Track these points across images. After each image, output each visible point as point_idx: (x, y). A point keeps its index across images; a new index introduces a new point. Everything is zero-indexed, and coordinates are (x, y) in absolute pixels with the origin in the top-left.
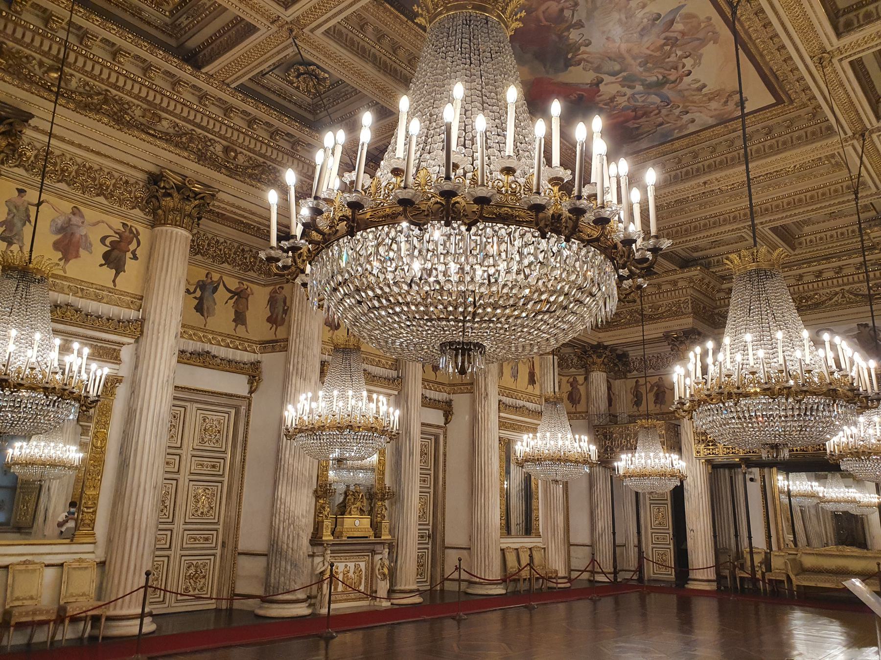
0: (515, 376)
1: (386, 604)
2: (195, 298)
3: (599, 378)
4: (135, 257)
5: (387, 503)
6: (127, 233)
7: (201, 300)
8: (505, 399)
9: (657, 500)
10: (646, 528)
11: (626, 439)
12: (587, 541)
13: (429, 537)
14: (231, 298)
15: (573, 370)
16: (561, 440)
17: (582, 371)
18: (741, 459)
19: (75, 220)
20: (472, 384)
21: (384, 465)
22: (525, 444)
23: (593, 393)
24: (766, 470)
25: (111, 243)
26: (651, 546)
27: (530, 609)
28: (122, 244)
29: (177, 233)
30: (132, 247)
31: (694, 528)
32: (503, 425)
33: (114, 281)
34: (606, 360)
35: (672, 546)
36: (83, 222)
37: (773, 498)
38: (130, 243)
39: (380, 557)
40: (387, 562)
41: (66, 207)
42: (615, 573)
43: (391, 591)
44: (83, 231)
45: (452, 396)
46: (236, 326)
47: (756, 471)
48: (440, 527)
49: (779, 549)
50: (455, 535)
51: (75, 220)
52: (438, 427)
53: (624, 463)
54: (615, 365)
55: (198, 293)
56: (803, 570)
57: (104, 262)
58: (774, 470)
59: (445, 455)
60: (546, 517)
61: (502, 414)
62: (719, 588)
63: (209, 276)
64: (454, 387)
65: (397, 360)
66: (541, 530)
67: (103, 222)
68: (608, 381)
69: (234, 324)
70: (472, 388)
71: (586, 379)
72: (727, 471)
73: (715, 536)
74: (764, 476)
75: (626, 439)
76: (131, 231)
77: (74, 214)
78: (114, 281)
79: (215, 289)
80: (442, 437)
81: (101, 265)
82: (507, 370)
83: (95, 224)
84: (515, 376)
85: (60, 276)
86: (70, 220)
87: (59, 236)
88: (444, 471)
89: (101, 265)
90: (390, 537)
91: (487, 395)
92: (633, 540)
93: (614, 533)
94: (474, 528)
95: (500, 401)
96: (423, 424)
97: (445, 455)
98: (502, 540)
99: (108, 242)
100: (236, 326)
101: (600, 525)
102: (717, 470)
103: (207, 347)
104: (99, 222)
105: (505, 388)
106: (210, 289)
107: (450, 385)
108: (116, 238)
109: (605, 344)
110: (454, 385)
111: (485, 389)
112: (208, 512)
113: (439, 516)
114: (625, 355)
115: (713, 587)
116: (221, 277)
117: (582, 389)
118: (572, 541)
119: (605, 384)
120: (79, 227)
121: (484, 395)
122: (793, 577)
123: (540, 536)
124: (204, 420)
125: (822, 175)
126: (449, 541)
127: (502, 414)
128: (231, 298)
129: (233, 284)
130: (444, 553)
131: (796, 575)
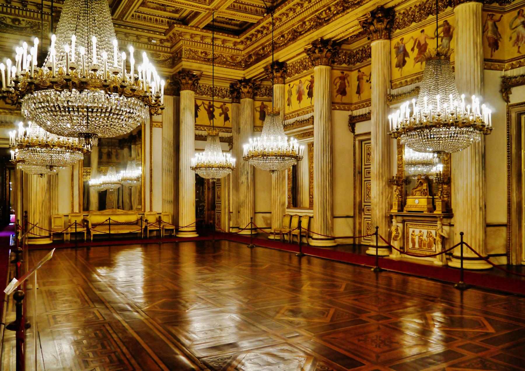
19: (300, 85)
51: (300, 85)
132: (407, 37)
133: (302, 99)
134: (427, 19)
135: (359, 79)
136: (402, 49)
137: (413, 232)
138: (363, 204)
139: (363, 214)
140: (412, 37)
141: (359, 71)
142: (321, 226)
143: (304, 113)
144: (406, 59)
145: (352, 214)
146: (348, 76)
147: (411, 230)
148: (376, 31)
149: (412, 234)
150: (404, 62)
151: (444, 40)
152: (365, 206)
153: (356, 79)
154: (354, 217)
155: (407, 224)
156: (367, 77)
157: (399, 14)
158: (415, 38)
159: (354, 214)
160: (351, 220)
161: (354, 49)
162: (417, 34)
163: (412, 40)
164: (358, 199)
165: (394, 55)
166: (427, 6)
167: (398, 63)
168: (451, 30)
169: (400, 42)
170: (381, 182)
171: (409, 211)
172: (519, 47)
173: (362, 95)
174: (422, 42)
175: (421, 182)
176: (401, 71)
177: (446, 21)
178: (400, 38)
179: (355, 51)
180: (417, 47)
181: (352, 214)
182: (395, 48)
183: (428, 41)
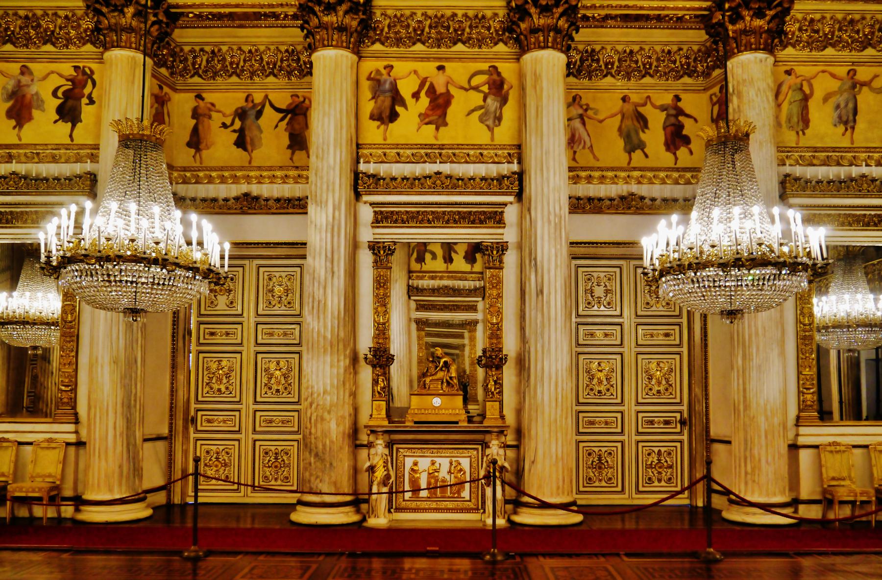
2: (234, 131)
4: (92, 102)
6: (80, 77)
7: (241, 132)
13: (683, 422)
14: (282, 119)
19: (25, 80)
25: (64, 93)
28: (76, 91)
29: (116, 56)
30: (87, 91)
33: (71, 136)
36: (32, 80)
38: (84, 86)
41: (14, 68)
44: (34, 89)
46: (293, 154)
51: (25, 80)
55: (238, 124)
57: (58, 117)
63: (250, 99)
67: (53, 72)
69: (289, 151)
76: (84, 73)
77: (22, 73)
78: (71, 136)
79: (259, 114)
81: (55, 122)
83: (45, 78)
85: (18, 145)
86: (19, 81)
87: (9, 104)
89: (55, 122)
99: (60, 94)
100: (293, 154)
103: (244, 188)
104: (48, 74)
106: (252, 114)
108: (68, 86)
112: (667, 390)
116: (266, 97)
120: (28, 86)
124: (270, 279)
128: (282, 119)
129: (282, 99)
130: (708, 450)
132: (401, 68)
133: (30, 118)
134: (410, 49)
135: (196, 114)
136: (387, 86)
137: (416, 464)
138: (193, 406)
139: (192, 430)
140: (415, 72)
141: (199, 97)
142: (120, 467)
143: (38, 158)
144: (398, 109)
145: (165, 431)
146: (169, 99)
147: (409, 462)
148: (341, 29)
149: (412, 470)
150: (393, 116)
151: (489, 100)
152: (198, 410)
153: (190, 114)
154: (169, 439)
155: (397, 449)
156: (224, 115)
157: (384, 14)
158: (423, 74)
159: (171, 431)
160: (161, 445)
161: (187, 44)
162: (428, 69)
163: (413, 76)
164: (181, 394)
165: (366, 93)
166: (413, 24)
167: (375, 112)
168: (505, 87)
169: (384, 72)
170: (342, 358)
171: (416, 423)
172: (575, 152)
173: (205, 153)
174: (440, 89)
175: (445, 362)
176: (386, 130)
177: (495, 68)
178: (386, 63)
179: (187, 49)
180: (428, 94)
181: (165, 431)
182: (369, 78)
183: (453, 91)
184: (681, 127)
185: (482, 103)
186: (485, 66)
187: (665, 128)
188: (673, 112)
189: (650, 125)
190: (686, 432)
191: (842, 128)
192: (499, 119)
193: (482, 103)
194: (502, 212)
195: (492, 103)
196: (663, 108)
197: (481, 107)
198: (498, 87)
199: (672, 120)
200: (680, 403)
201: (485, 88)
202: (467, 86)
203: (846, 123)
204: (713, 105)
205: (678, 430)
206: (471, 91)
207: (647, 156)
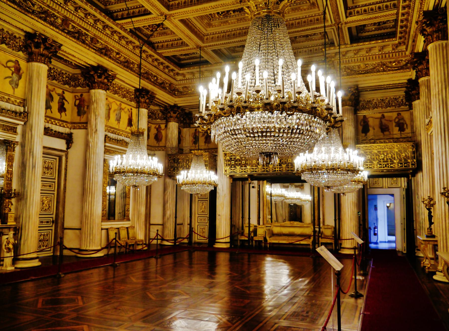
0: (118, 120)
1: (10, 268)
3: (173, 126)
5: (13, 201)
8: (110, 135)
9: (202, 198)
10: (195, 214)
11: (186, 163)
12: (160, 222)
13: (53, 222)
15: (159, 120)
16: (144, 161)
17: (164, 121)
18: (249, 175)
20: (86, 123)
21: (11, 174)
22: (115, 162)
23: (170, 135)
24: (261, 182)
26: (197, 224)
27: (114, 267)
31: (221, 214)
32: (107, 151)
34: (178, 116)
35: (208, 224)
37: (263, 197)
39: (7, 237)
40: (12, 241)
42: (175, 239)
43: (15, 260)
45: (72, 131)
47: (256, 182)
48: (61, 216)
49: (264, 224)
50: (70, 221)
52: (61, 151)
53: (182, 176)
54: (184, 119)
56: (273, 235)
58: (265, 182)
59: (66, 169)
60: (134, 210)
61: (107, 144)
62: (231, 246)
64: (74, 125)
65: (24, 100)
66: (130, 217)
68: (179, 129)
70: (87, 126)
71: (166, 126)
72: (241, 182)
73: (231, 218)
74: (259, 185)
75: (186, 163)
80: (64, 158)
82: (113, 116)
84: (118, 120)
88: (65, 180)
90: (14, 223)
91: (96, 130)
92: (187, 221)
93: (176, 217)
94: (84, 216)
95: (106, 135)
96: (44, 147)
97: (66, 169)
98: (103, 223)
101: (168, 213)
102: (236, 182)
105: (111, 128)
107: (72, 123)
109: (179, 105)
110: (74, 123)
111: (96, 127)
113: (61, 209)
114: (190, 114)
115: (228, 246)
117: (163, 132)
118: (152, 222)
119: (177, 130)
121: (94, 130)
122: (268, 238)
123: (129, 220)
125: (305, 10)
126: (66, 225)
127: (107, 144)
130: (63, 232)
131: (270, 237)
151: (14, 75)
168: (21, 71)
184: (63, 104)
185: (11, 75)
186: (14, 59)
187: (59, 103)
188: (61, 97)
189: (54, 100)
190: (54, 226)
191: (117, 122)
192: (17, 85)
193: (11, 75)
194: (16, 128)
195: (15, 77)
196: (59, 95)
197: (10, 77)
198: (18, 70)
199: (61, 100)
200: (52, 214)
201: (13, 69)
202: (5, 65)
203: (118, 120)
204: (76, 100)
205: (51, 225)
206: (7, 68)
207: (52, 112)
